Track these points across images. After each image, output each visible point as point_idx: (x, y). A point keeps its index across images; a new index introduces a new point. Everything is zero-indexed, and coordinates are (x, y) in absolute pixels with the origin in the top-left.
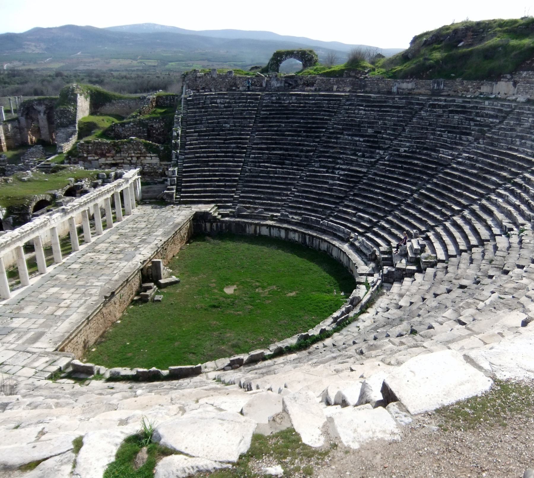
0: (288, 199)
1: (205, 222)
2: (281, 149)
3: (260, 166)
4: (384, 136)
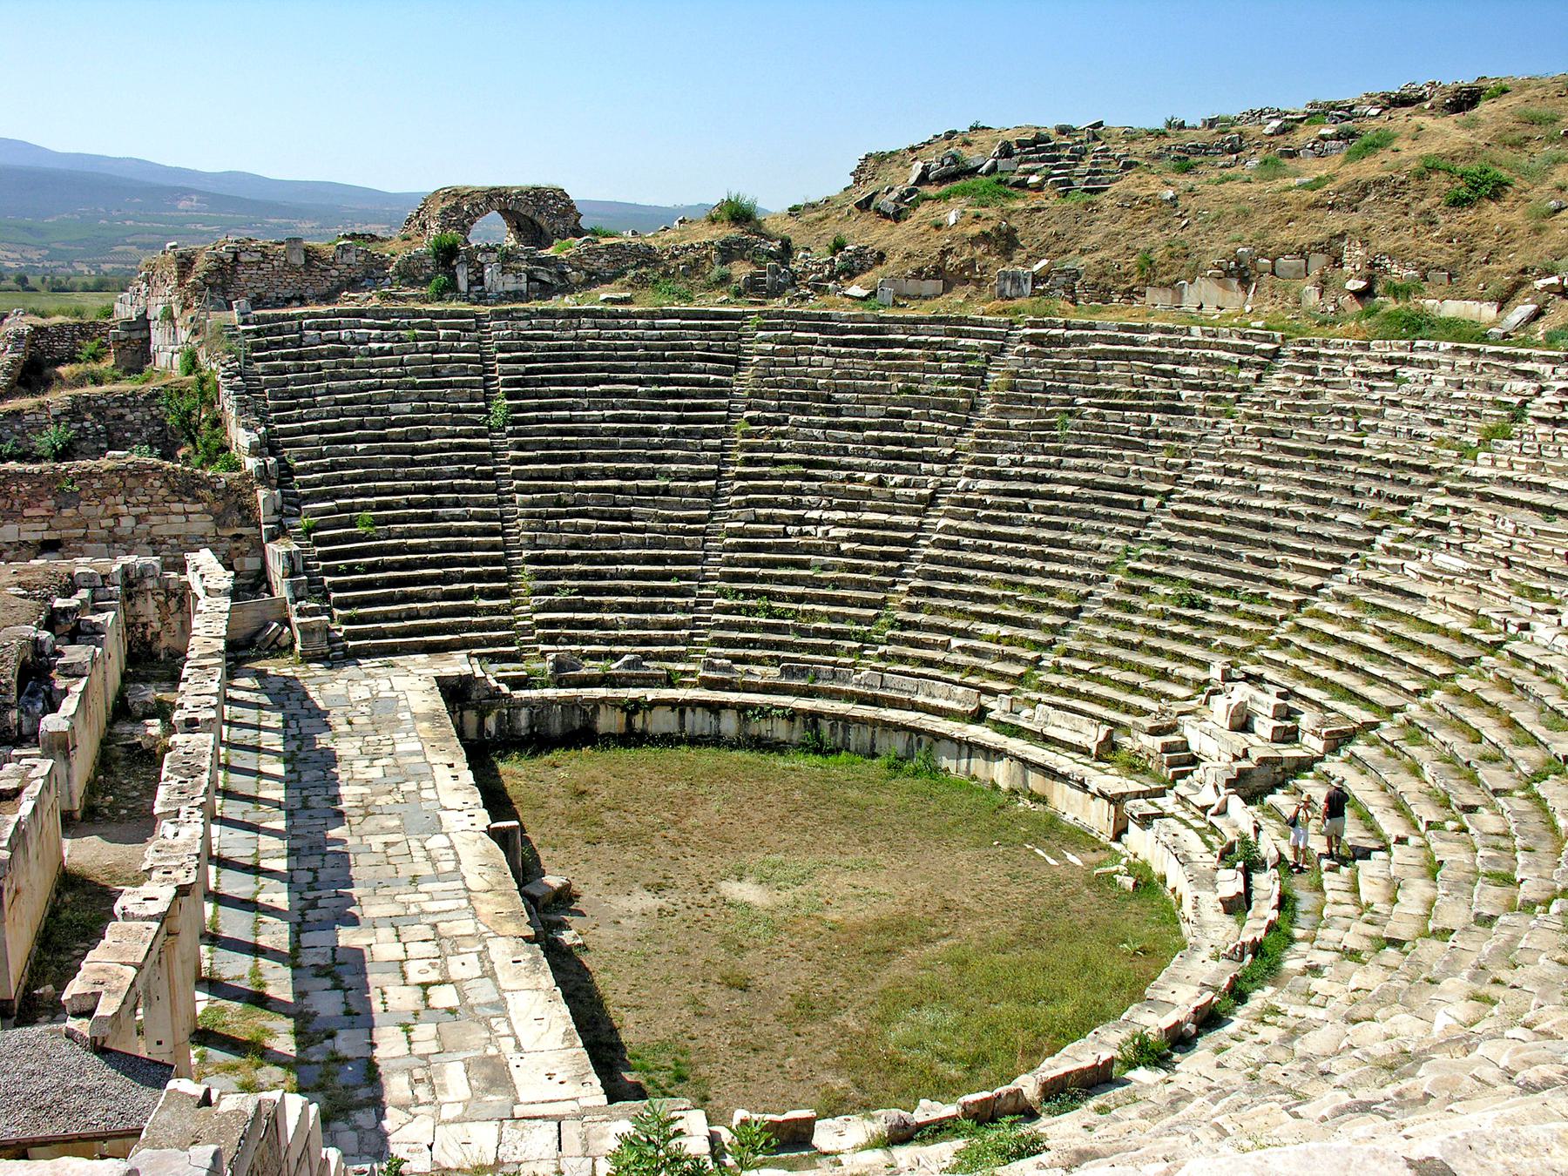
0: (694, 620)
1: (462, 710)
2: (604, 475)
3: (559, 529)
4: (925, 423)
